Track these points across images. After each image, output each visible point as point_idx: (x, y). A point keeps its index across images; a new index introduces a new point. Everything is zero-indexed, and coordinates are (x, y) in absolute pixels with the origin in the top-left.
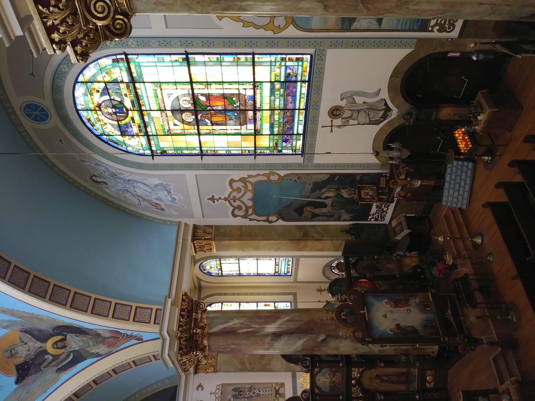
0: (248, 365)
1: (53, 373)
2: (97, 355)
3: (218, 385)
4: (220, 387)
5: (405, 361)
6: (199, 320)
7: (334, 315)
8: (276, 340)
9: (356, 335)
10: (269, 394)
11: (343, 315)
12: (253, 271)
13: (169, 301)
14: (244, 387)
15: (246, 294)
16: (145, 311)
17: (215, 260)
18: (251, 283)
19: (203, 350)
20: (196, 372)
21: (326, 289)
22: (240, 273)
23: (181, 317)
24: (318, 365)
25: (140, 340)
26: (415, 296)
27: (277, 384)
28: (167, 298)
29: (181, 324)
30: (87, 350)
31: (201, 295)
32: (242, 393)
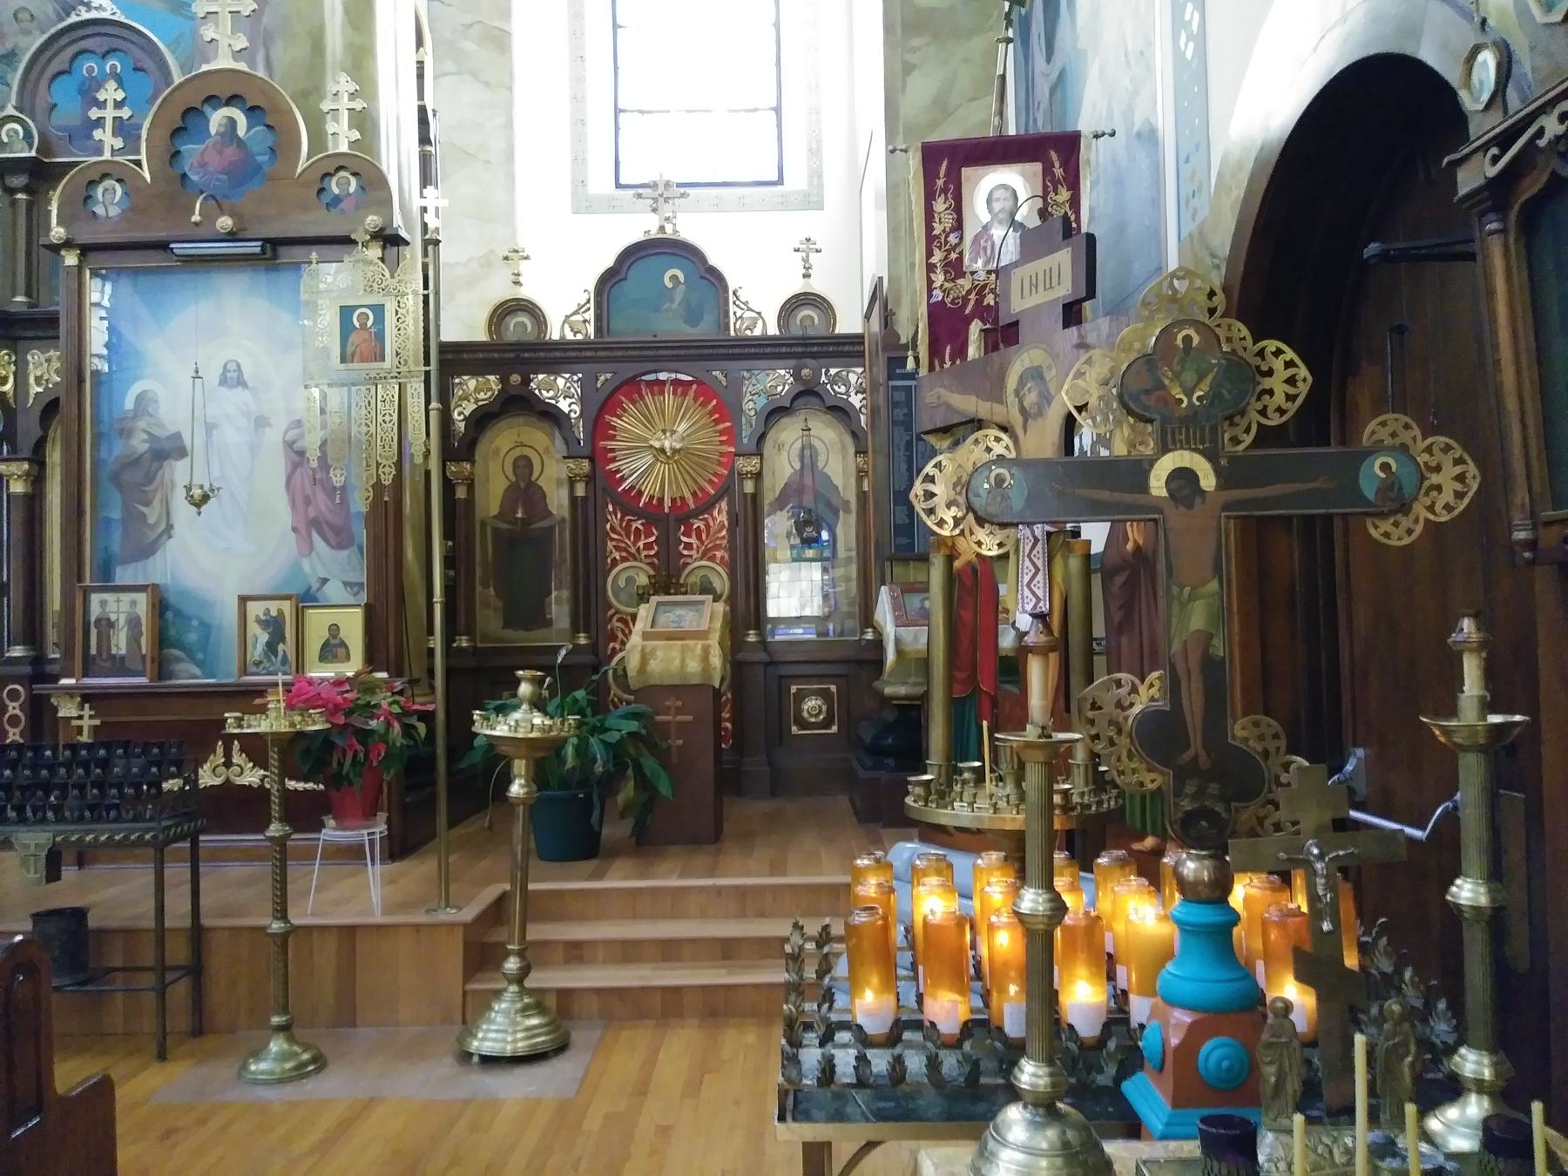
7: (223, 62)
9: (108, 183)
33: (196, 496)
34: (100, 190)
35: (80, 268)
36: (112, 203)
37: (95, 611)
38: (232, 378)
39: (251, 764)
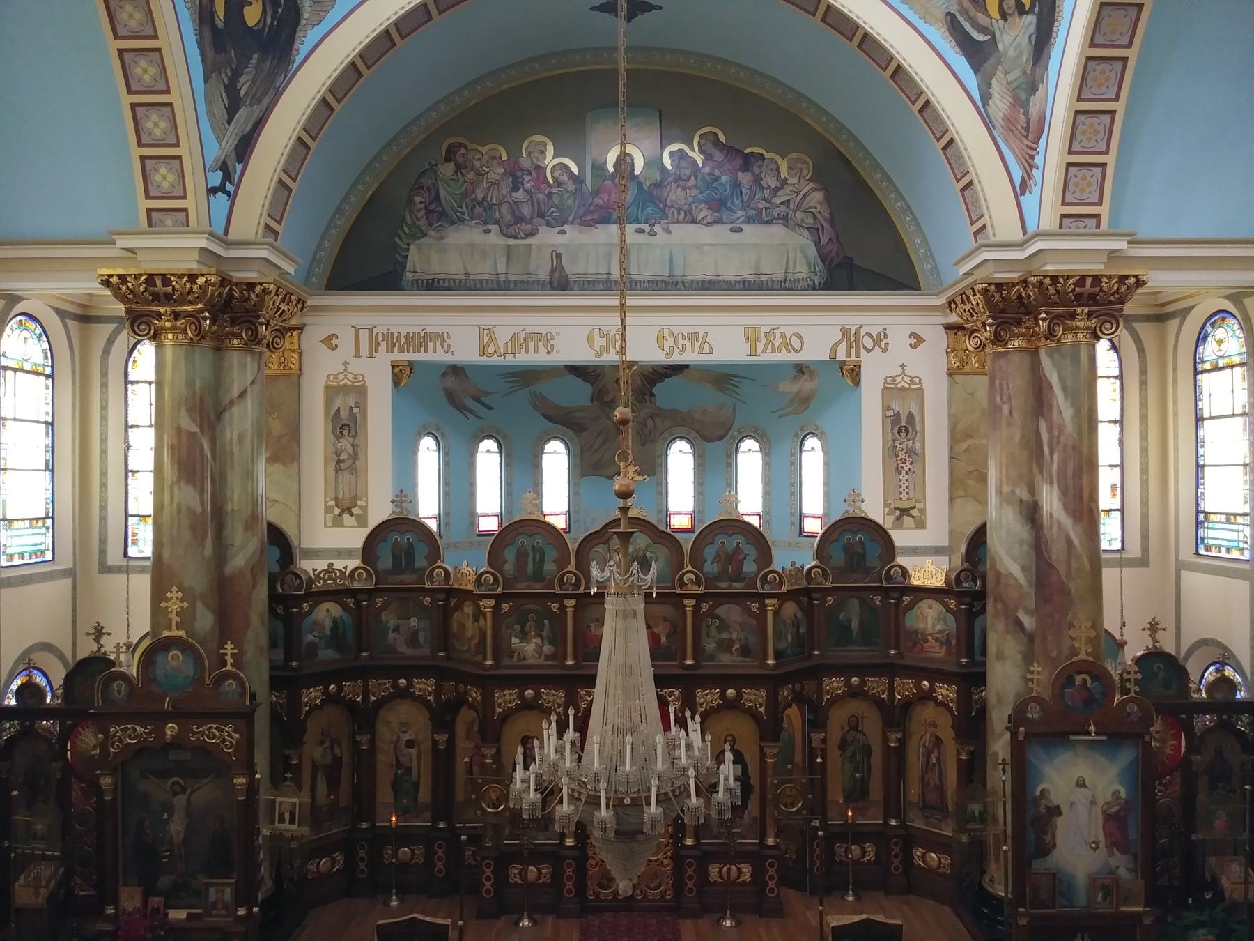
0: (964, 446)
1: (946, 6)
2: (986, 97)
3: (920, 379)
4: (916, 384)
5: (968, 810)
6: (1071, 323)
7: (1083, 656)
8: (1020, 513)
10: (901, 493)
11: (1085, 681)
12: (1209, 455)
13: (1121, 245)
14: (917, 438)
15: (1144, 437)
16: (1093, 189)
17: (1244, 349)
18: (1176, 448)
19: (997, 339)
20: (948, 328)
21: (1156, 644)
22: (1203, 419)
23: (1078, 278)
24: (963, 606)
25: (1022, 189)
26: (1134, 870)
27: (923, 511)
28: (1129, 238)
29: (1061, 281)
30: (996, 69)
31: (1142, 321)
32: (903, 434)
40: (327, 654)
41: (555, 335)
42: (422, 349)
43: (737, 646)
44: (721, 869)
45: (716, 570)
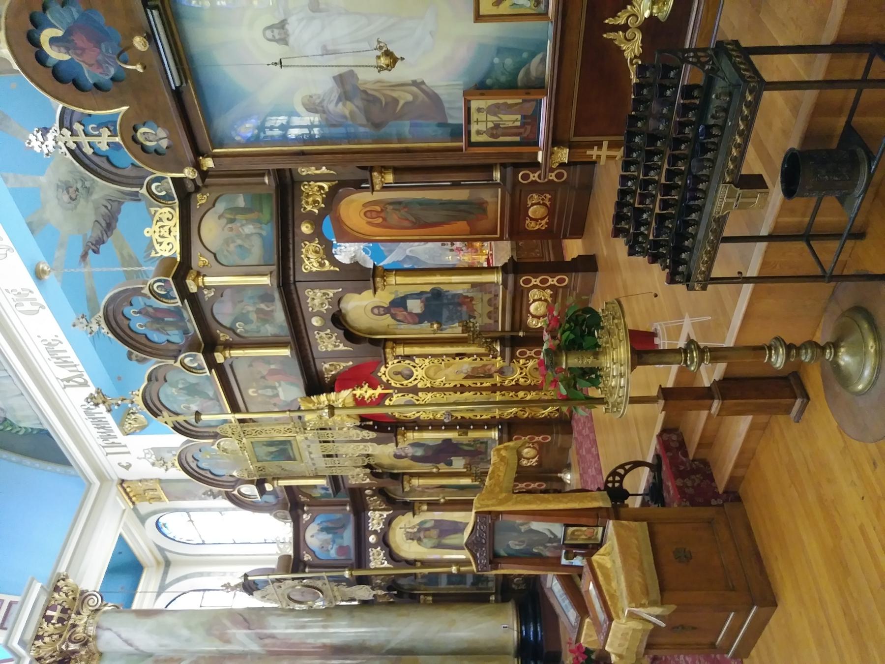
33: (387, 62)
34: (148, 144)
35: (214, 156)
36: (156, 134)
37: (484, 138)
38: (279, 34)
39: (629, 7)
40: (348, 537)
41: (41, 339)
42: (103, 420)
43: (263, 306)
44: (534, 316)
45: (176, 332)
